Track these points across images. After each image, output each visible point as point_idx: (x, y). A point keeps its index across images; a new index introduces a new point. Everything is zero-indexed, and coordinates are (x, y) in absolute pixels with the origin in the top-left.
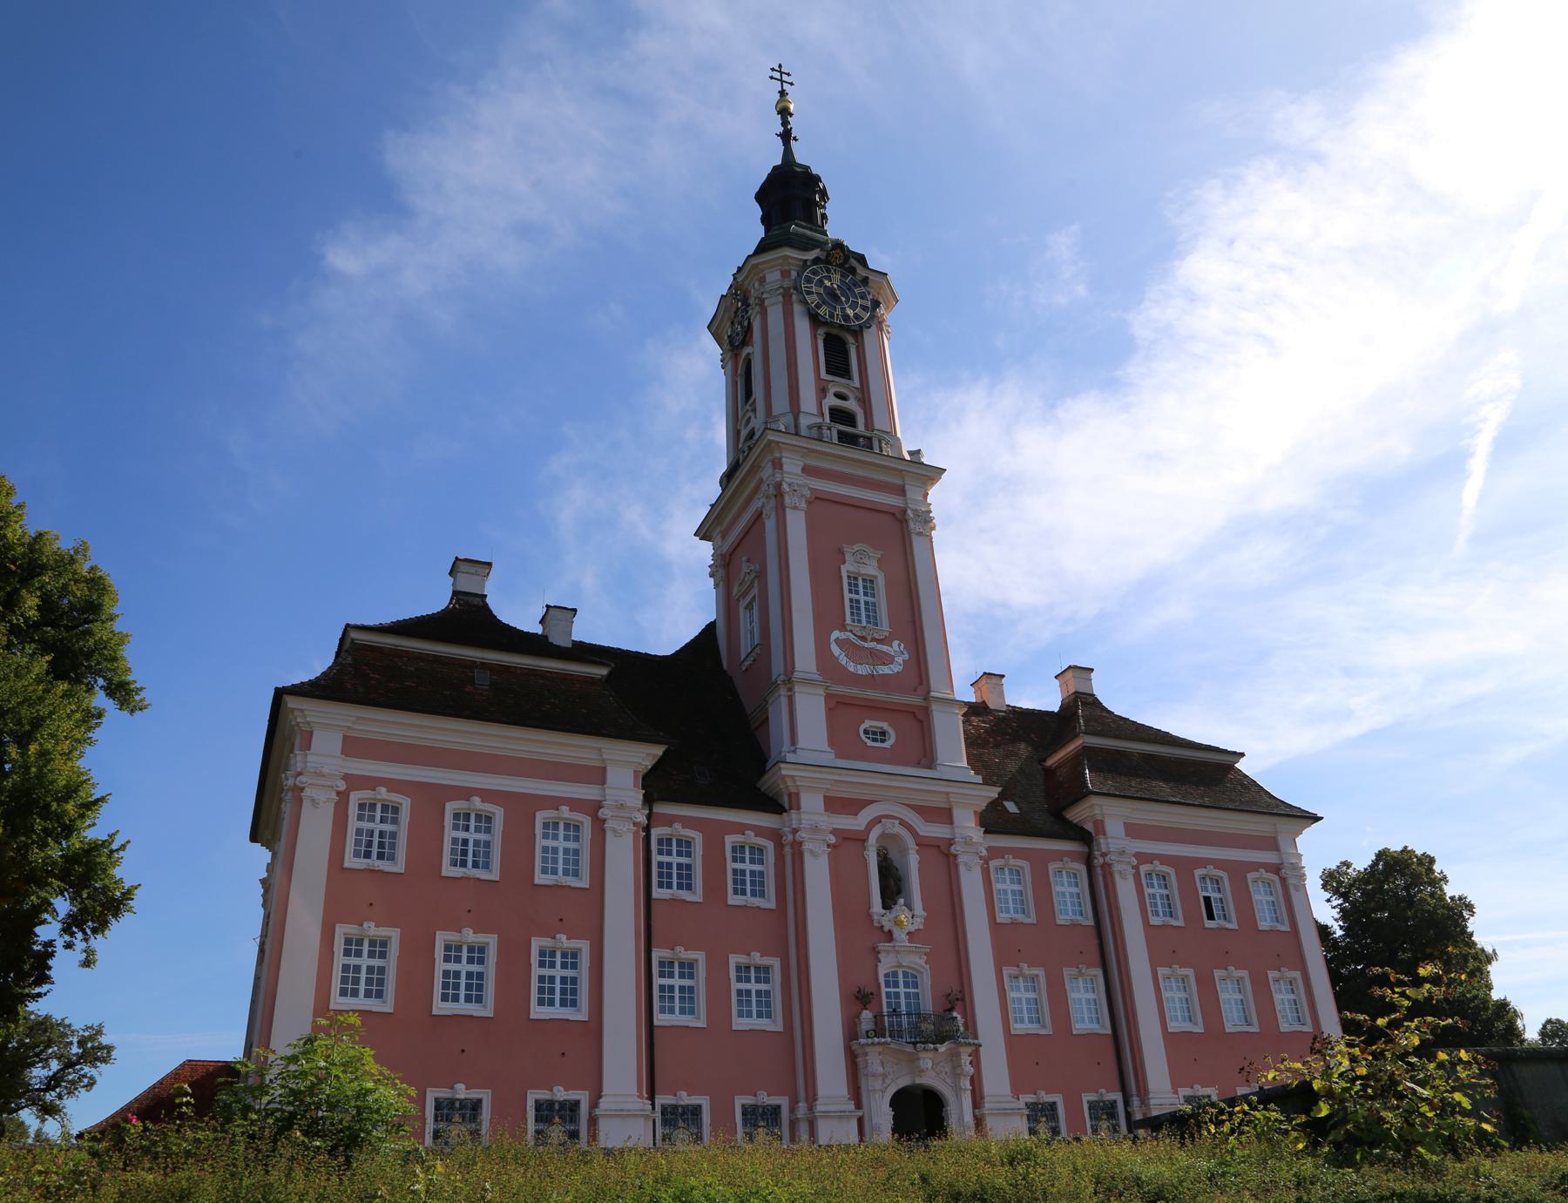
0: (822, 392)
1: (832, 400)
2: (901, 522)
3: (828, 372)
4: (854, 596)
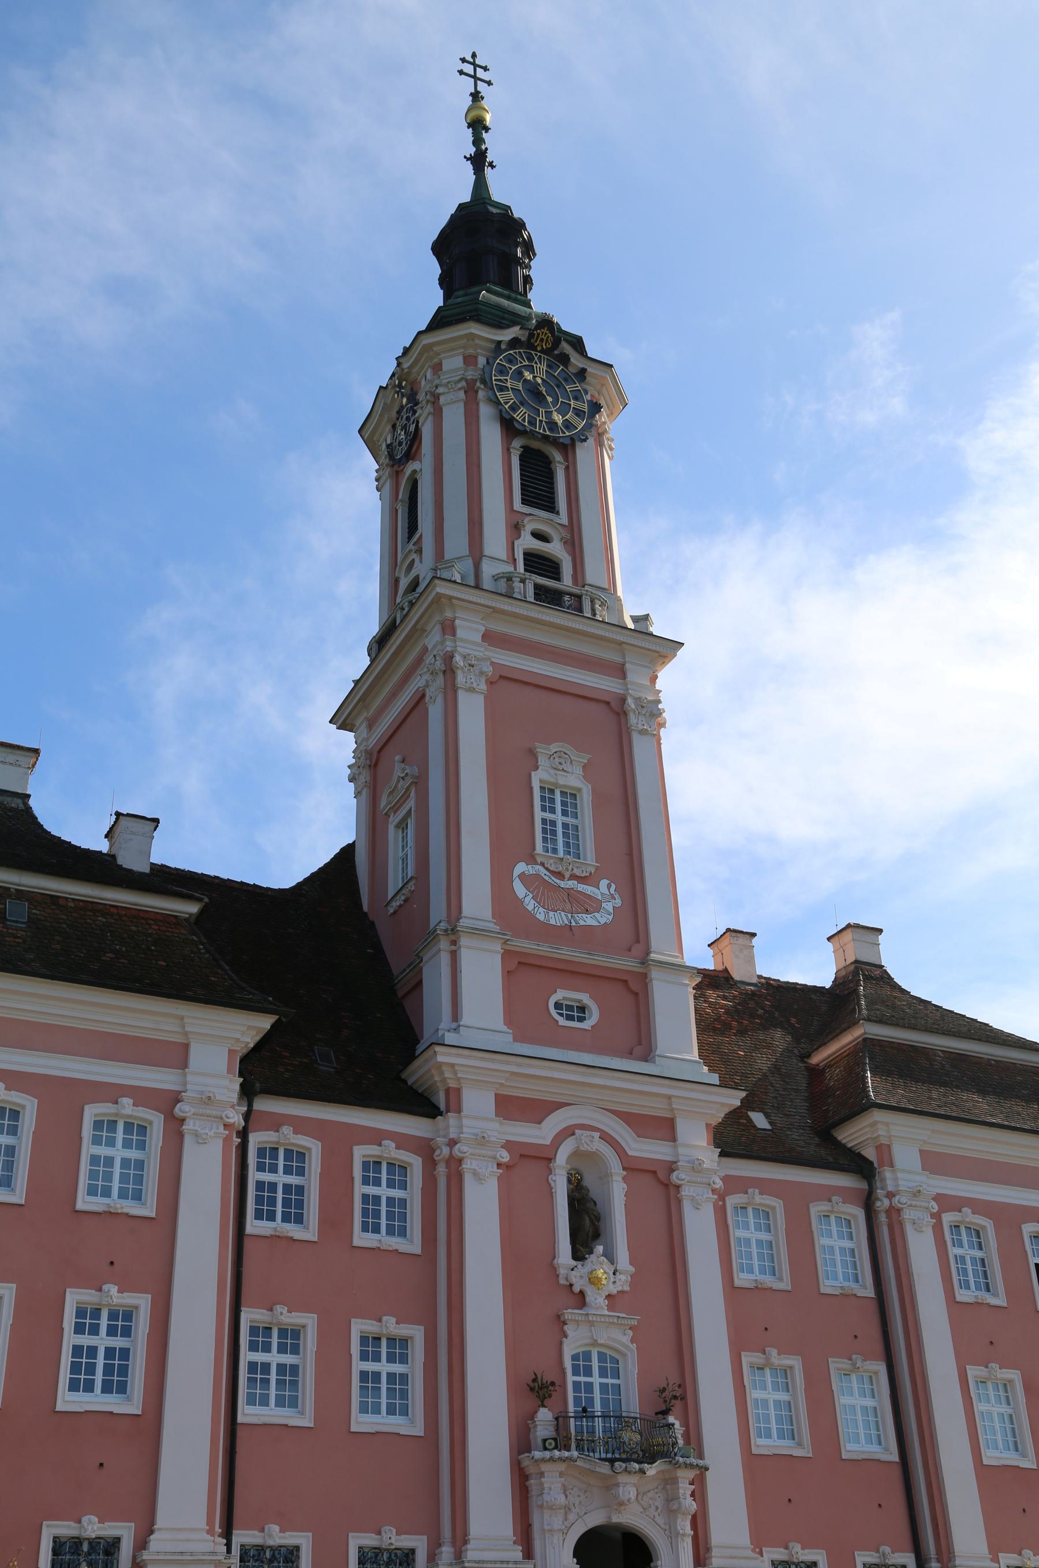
0: (515, 529)
1: (527, 542)
2: (618, 714)
3: (524, 502)
4: (548, 816)
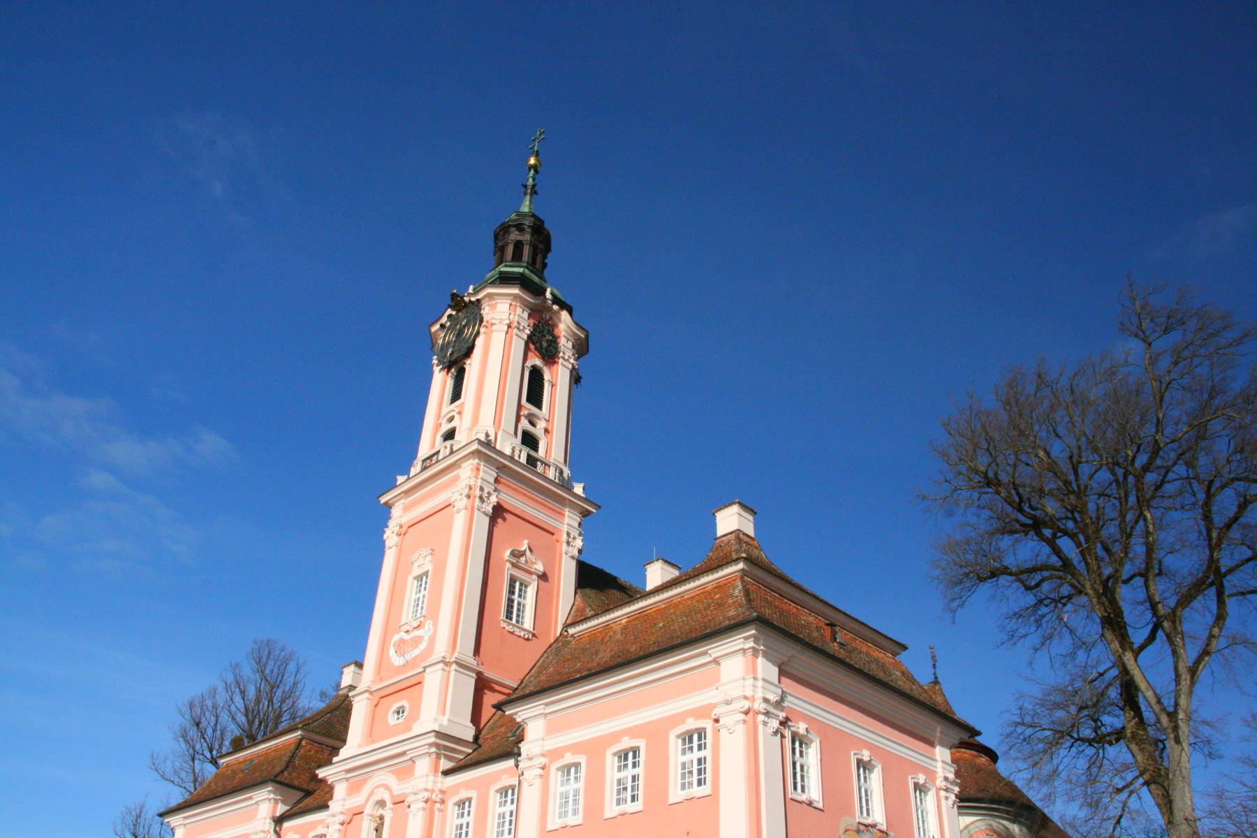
3: (528, 400)
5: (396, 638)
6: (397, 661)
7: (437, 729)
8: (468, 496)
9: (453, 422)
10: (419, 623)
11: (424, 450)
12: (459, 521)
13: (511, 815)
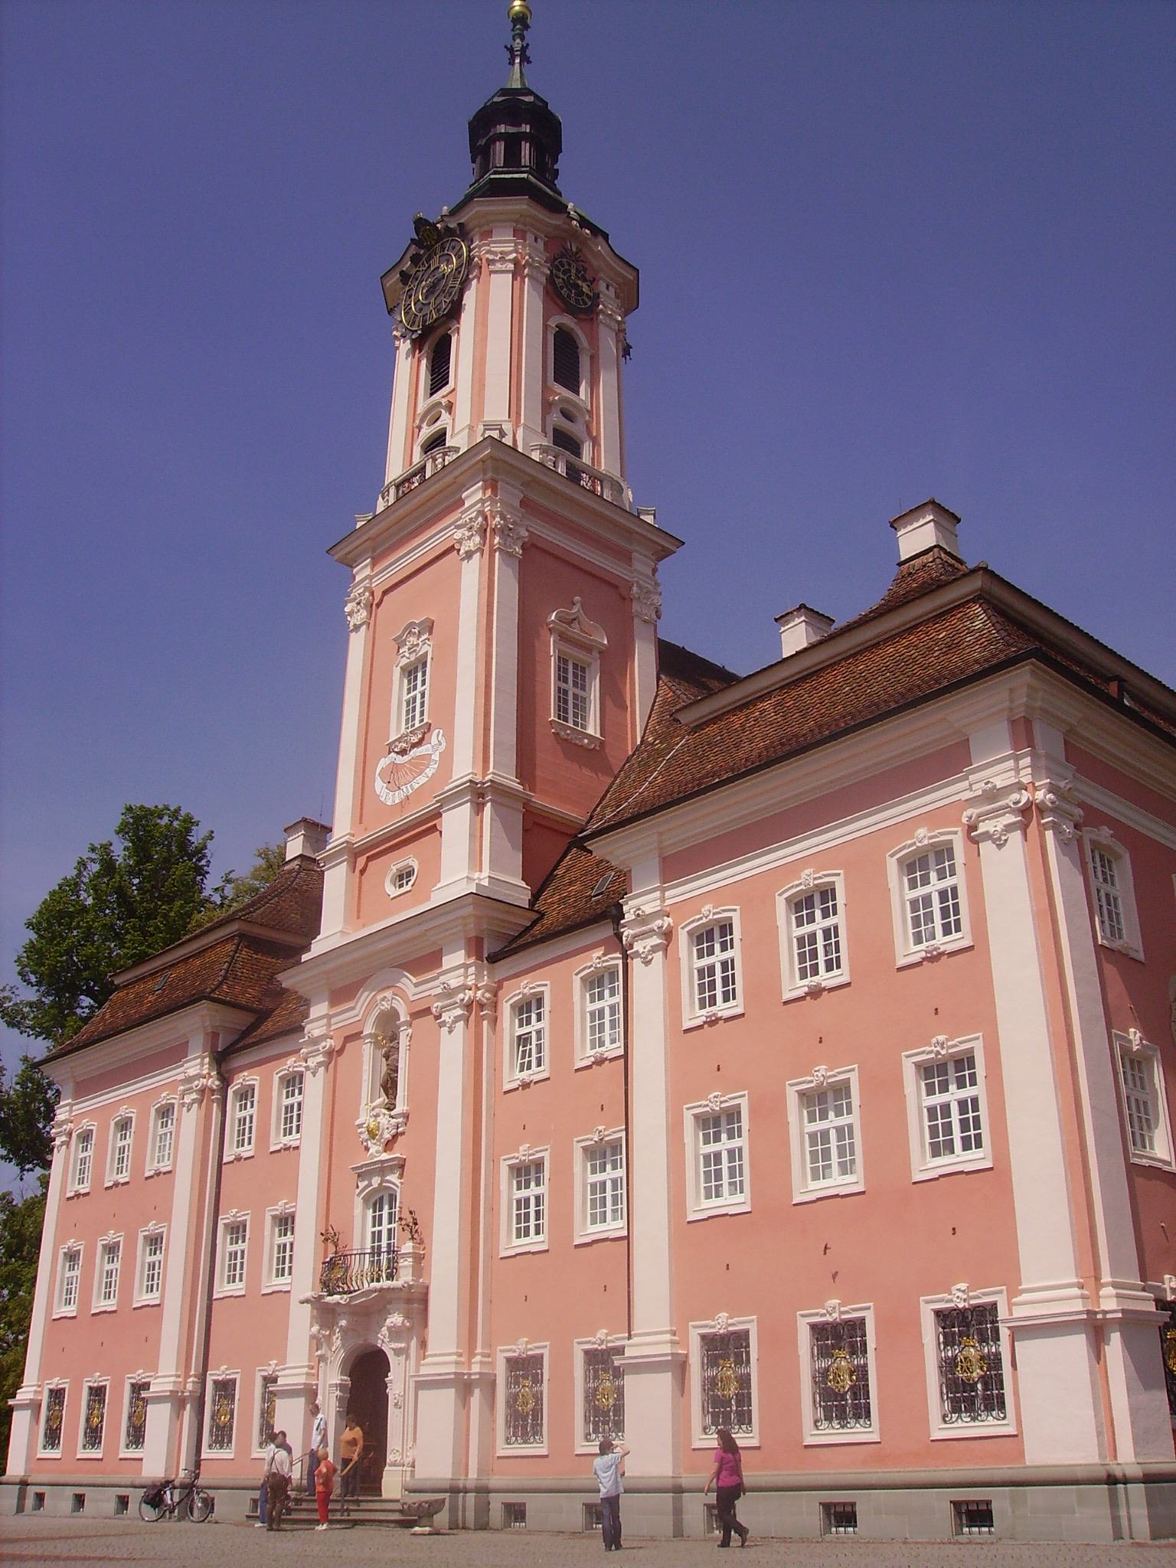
5: (384, 763)
6: (390, 798)
7: (474, 891)
8: (483, 531)
9: (438, 423)
10: (420, 736)
11: (395, 469)
12: (471, 574)
13: (613, 1012)
